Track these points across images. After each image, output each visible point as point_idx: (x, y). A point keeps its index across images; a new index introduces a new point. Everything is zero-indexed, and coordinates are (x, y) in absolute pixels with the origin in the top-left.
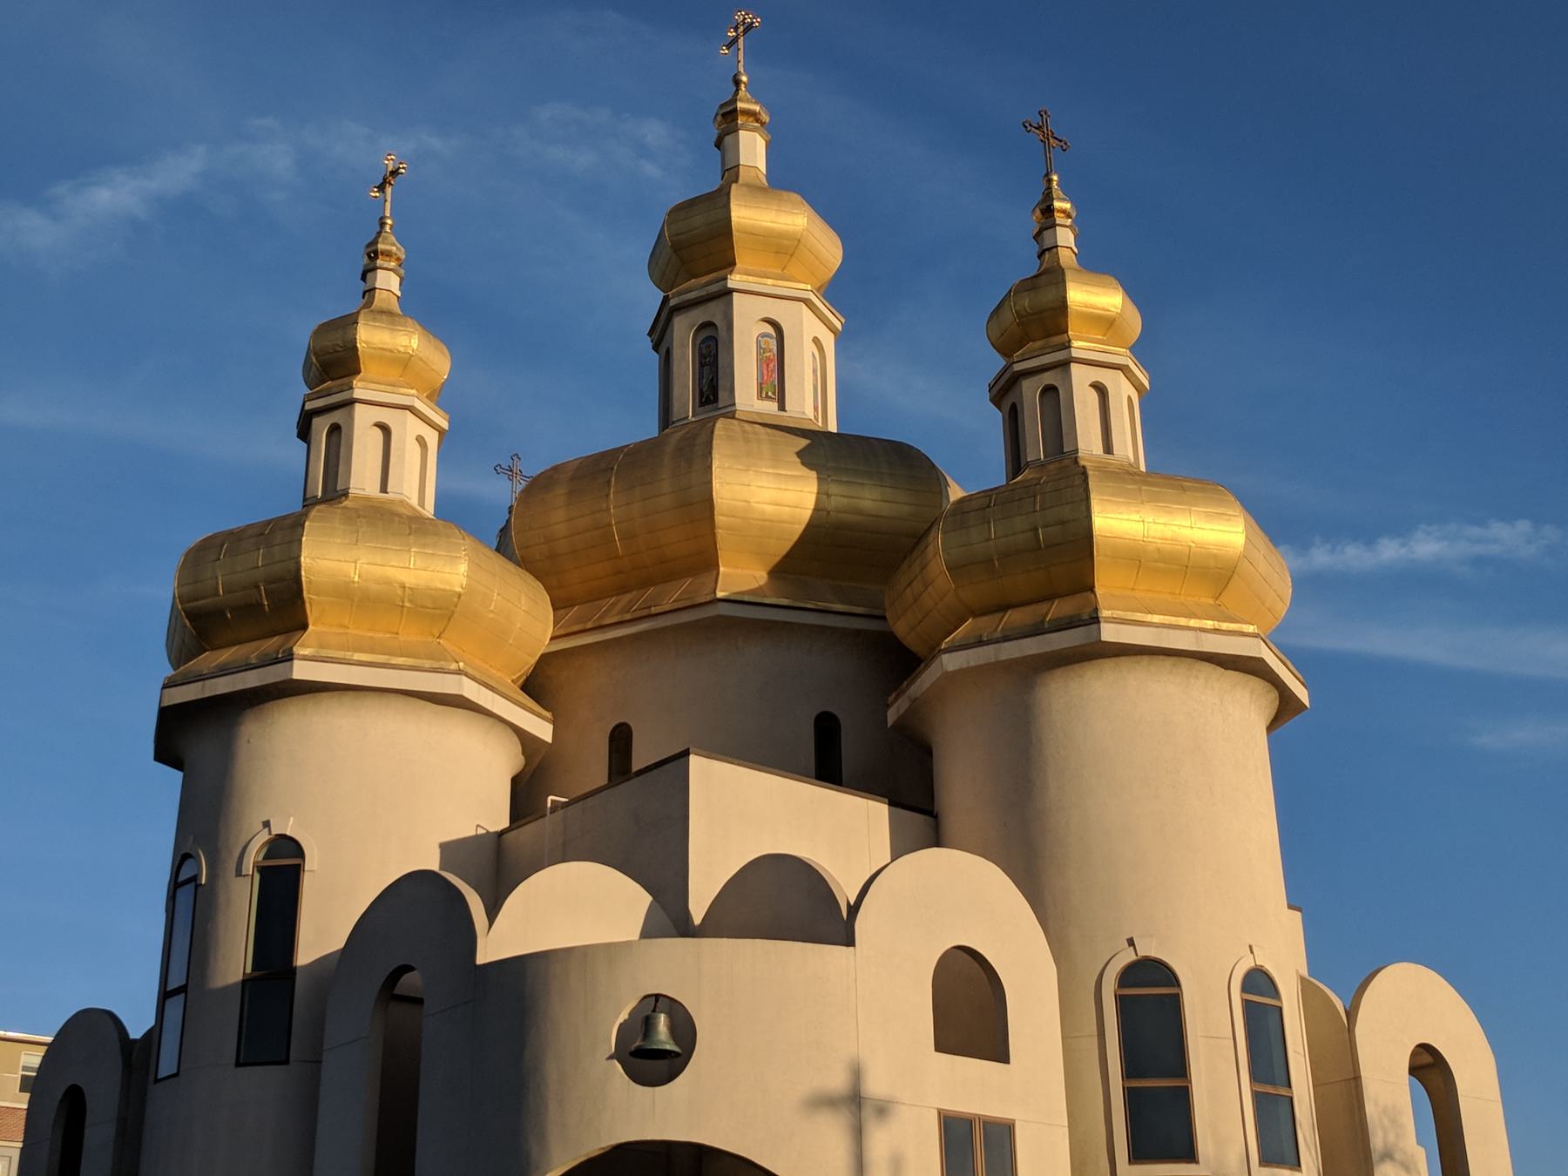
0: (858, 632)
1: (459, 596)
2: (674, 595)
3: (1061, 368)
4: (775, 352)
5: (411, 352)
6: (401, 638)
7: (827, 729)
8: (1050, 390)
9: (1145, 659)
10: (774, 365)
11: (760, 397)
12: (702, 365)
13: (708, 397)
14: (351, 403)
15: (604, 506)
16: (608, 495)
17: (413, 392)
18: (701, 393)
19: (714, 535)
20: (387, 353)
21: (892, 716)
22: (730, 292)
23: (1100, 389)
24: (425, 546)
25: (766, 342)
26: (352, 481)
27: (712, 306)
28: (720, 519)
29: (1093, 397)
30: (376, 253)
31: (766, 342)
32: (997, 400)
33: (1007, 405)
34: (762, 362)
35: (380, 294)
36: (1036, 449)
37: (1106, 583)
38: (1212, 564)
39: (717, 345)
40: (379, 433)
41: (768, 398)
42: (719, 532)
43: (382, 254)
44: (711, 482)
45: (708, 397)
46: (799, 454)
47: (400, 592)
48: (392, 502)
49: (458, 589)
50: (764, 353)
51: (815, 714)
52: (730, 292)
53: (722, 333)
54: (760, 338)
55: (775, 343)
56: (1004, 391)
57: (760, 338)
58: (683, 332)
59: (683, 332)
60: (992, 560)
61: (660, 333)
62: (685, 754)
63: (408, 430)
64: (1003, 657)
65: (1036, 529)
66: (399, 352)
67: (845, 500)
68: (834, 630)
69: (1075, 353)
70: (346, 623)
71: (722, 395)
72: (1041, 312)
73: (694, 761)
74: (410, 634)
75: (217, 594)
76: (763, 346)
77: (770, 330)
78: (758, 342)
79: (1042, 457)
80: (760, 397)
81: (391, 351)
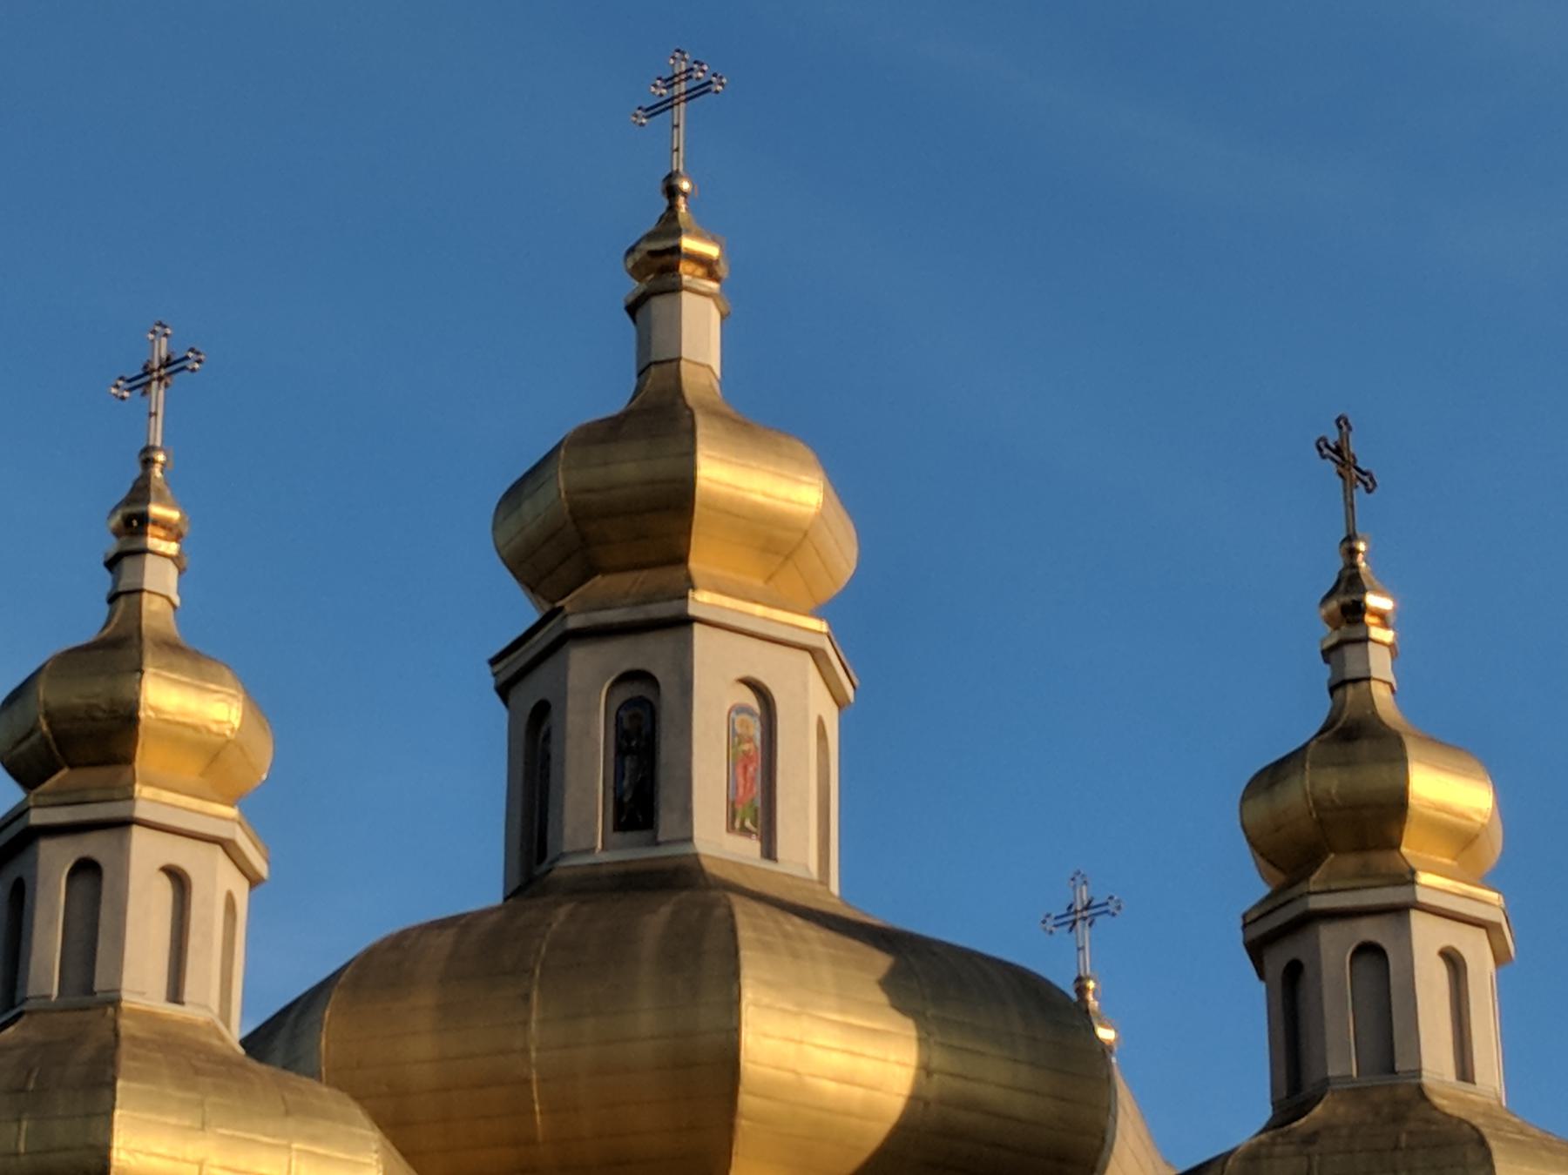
4: (758, 743)
5: (228, 733)
10: (755, 769)
17: (232, 812)
20: (189, 733)
22: (686, 622)
25: (743, 721)
31: (743, 723)
34: (737, 761)
35: (150, 602)
43: (156, 523)
48: (193, 1026)
50: (740, 743)
53: (668, 697)
54: (733, 714)
55: (758, 724)
57: (733, 714)
66: (209, 731)
76: (739, 730)
77: (749, 699)
78: (730, 723)
79: (1355, 1073)
81: (195, 728)
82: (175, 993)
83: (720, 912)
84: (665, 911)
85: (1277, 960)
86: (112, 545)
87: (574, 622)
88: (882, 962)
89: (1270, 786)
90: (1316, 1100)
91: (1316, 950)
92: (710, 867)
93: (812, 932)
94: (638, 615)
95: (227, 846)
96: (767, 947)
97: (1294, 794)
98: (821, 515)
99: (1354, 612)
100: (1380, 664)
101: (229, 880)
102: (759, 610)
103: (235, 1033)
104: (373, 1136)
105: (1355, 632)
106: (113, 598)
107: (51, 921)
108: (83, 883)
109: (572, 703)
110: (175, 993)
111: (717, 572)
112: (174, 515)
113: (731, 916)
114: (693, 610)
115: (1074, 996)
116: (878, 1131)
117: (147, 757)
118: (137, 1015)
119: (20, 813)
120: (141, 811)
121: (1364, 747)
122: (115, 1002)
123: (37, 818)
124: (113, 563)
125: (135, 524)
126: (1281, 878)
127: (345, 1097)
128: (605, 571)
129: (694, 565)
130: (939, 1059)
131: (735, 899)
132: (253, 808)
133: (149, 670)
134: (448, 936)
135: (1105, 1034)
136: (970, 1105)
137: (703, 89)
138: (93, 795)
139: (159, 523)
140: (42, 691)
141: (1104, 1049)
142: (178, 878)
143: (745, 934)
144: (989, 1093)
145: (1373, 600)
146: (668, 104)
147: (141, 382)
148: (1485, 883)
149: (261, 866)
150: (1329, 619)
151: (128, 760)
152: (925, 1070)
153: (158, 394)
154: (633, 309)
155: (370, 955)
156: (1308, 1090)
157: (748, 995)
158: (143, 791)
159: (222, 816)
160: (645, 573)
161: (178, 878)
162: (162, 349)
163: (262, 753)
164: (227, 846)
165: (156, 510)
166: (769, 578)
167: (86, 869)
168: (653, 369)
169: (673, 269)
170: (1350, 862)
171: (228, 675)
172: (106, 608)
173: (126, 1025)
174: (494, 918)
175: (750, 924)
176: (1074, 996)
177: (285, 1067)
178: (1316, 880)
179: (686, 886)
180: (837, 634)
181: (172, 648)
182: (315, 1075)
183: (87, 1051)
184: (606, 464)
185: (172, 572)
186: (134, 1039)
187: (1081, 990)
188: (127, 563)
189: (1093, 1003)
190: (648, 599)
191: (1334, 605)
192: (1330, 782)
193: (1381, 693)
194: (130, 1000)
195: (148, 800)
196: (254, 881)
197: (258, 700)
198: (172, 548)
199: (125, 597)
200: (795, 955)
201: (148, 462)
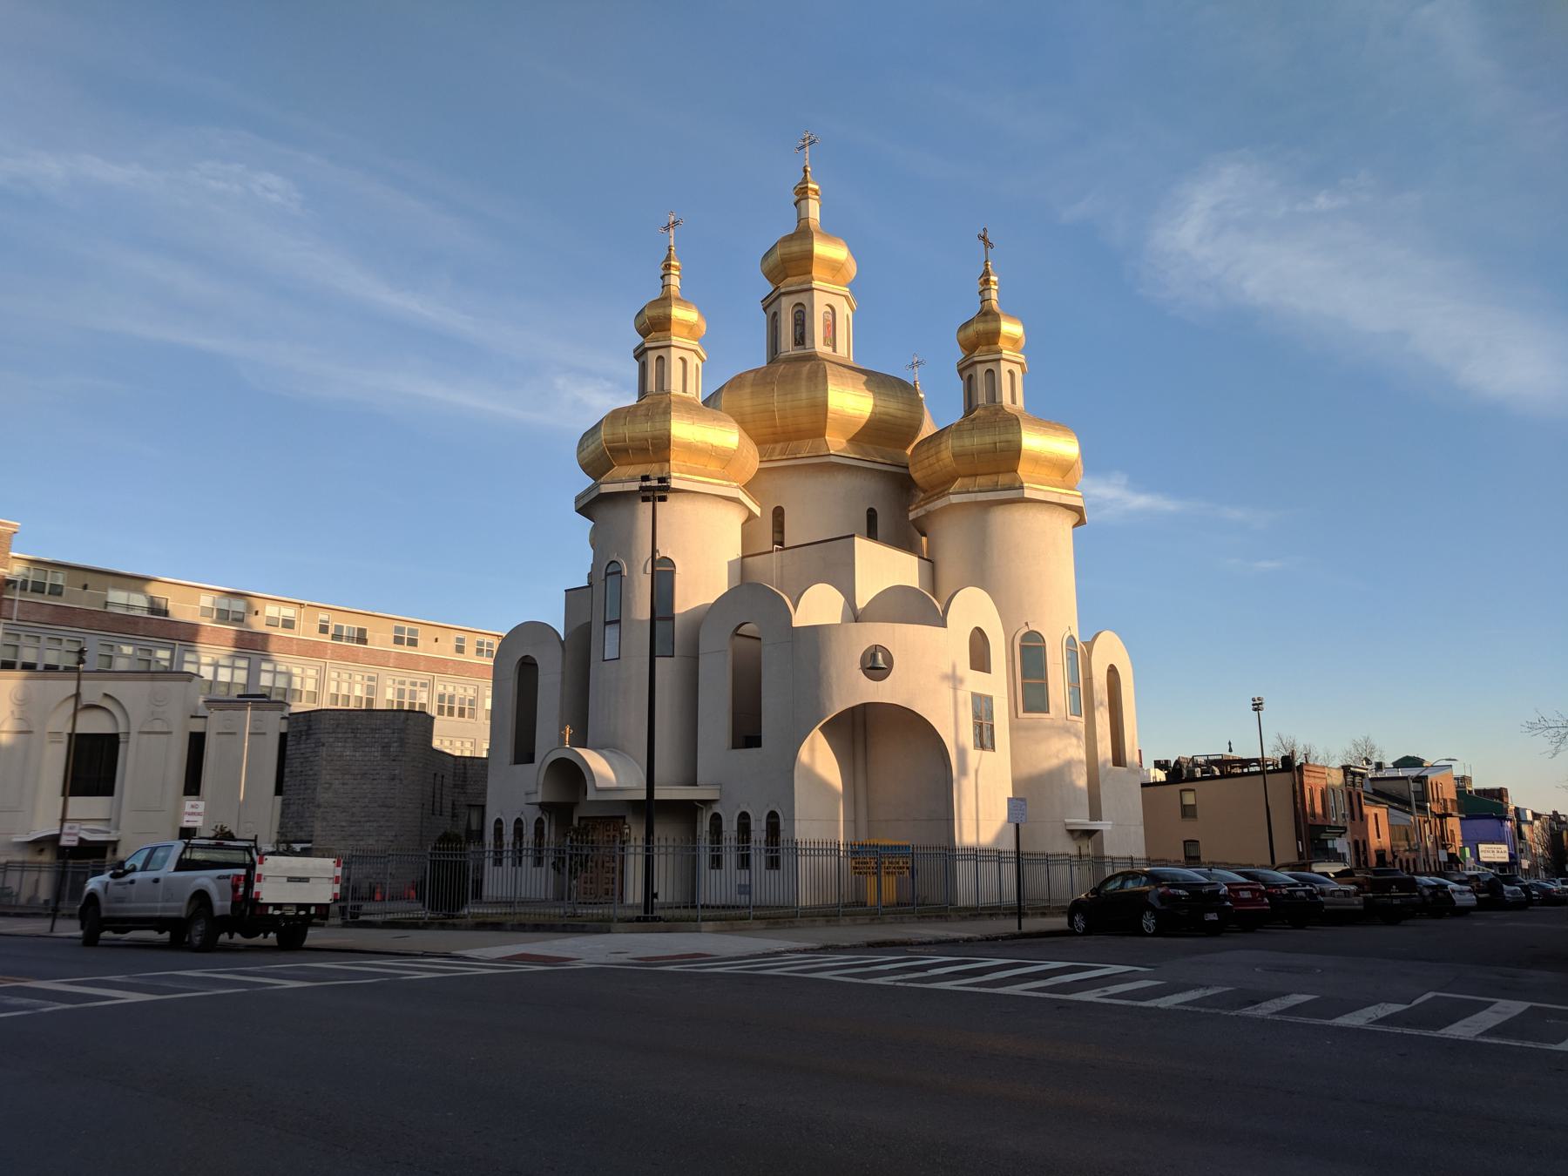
0: (886, 472)
1: (735, 451)
2: (806, 447)
3: (995, 363)
6: (708, 468)
7: (872, 515)
8: (990, 371)
9: (1038, 504)
11: (824, 345)
12: (796, 325)
13: (799, 342)
14: (669, 346)
15: (771, 401)
16: (773, 396)
17: (697, 343)
18: (795, 339)
19: (826, 422)
21: (912, 516)
23: (1011, 373)
24: (721, 426)
26: (672, 385)
27: (802, 295)
28: (829, 415)
29: (1008, 376)
30: (670, 265)
32: (961, 372)
33: (966, 374)
34: (826, 327)
36: (982, 398)
37: (1023, 470)
38: (1065, 463)
39: (804, 317)
40: (680, 363)
41: (828, 345)
42: (828, 420)
44: (827, 397)
45: (799, 342)
46: (866, 383)
47: (711, 448)
48: (688, 398)
49: (735, 448)
51: (868, 507)
52: (812, 289)
53: (808, 309)
56: (966, 369)
58: (786, 306)
59: (786, 306)
60: (974, 455)
61: (770, 303)
62: (853, 536)
63: (693, 361)
64: (979, 499)
65: (996, 443)
67: (883, 409)
68: (877, 470)
69: (1004, 356)
70: (686, 460)
71: (808, 342)
72: (986, 334)
73: (856, 538)
74: (713, 467)
75: (625, 441)
77: (829, 310)
80: (824, 345)
82: (685, 390)
83: (822, 366)
84: (808, 366)
85: (966, 374)
86: (662, 273)
87: (782, 290)
88: (865, 378)
89: (965, 328)
90: (975, 410)
91: (976, 371)
92: (819, 354)
93: (846, 370)
94: (799, 288)
95: (695, 352)
96: (834, 375)
97: (971, 331)
98: (847, 259)
99: (987, 281)
100: (994, 295)
101: (697, 361)
102: (832, 286)
103: (700, 401)
104: (736, 425)
105: (988, 287)
106: (663, 287)
107: (652, 370)
108: (660, 361)
109: (783, 312)
110: (685, 390)
111: (820, 276)
112: (678, 264)
113: (825, 367)
114: (814, 286)
115: (913, 384)
116: (864, 421)
117: (674, 329)
118: (675, 396)
119: (643, 344)
120: (673, 343)
121: (989, 317)
122: (670, 393)
123: (647, 345)
124: (662, 277)
125: (668, 267)
126: (967, 353)
127: (728, 416)
128: (791, 276)
129: (814, 274)
130: (879, 403)
131: (826, 363)
132: (703, 342)
133: (673, 306)
134: (753, 375)
135: (922, 395)
136: (887, 414)
137: (813, 142)
138: (661, 339)
139: (674, 266)
140: (647, 312)
141: (921, 399)
142: (683, 360)
143: (828, 372)
144: (891, 411)
145: (993, 278)
146: (804, 147)
147: (667, 228)
148: (1021, 352)
149: (705, 358)
150: (981, 283)
151: (670, 330)
152: (875, 405)
153: (672, 231)
154: (796, 204)
155: (733, 379)
156: (973, 407)
157: (829, 388)
158: (674, 338)
159: (694, 344)
160: (801, 277)
161: (683, 360)
162: (672, 219)
163: (704, 328)
164: (695, 352)
165: (673, 263)
166: (833, 277)
167: (660, 358)
168: (802, 221)
169: (807, 192)
170: (985, 348)
171: (693, 306)
172: (661, 290)
173: (672, 398)
174: (763, 370)
175: (830, 368)
176: (913, 384)
177: (714, 408)
178: (976, 353)
179: (813, 360)
180: (852, 291)
181: (678, 299)
182: (721, 410)
183: (663, 405)
184: (789, 247)
185: (678, 279)
186: (675, 402)
187: (915, 384)
188: (666, 277)
189: (918, 388)
190: (802, 283)
191: (982, 279)
192: (981, 327)
193: (994, 303)
194: (673, 392)
195: (675, 340)
196: (703, 361)
197: (702, 313)
198: (677, 273)
199: (666, 286)
200: (842, 377)
201: (670, 250)
